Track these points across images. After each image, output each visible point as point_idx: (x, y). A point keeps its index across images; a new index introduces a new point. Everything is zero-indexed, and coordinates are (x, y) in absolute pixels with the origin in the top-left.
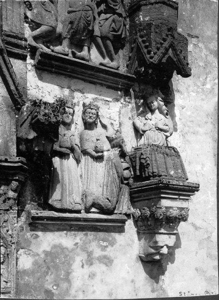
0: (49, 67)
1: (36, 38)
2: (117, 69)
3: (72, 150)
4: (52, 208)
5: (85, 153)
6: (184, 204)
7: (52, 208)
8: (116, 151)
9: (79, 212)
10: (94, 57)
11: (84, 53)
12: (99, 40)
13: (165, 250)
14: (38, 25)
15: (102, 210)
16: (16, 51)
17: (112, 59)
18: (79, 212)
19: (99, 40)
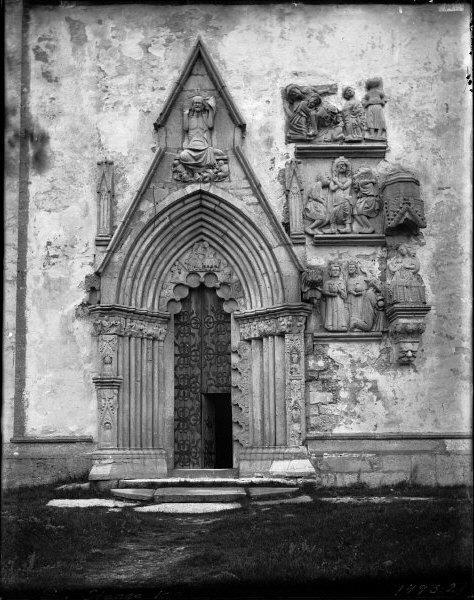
0: (319, 243)
1: (313, 229)
2: (373, 232)
3: (339, 293)
4: (327, 331)
5: (349, 293)
6: (420, 321)
7: (327, 331)
8: (371, 290)
9: (345, 332)
10: (355, 229)
11: (348, 228)
12: (358, 218)
13: (410, 354)
14: (313, 221)
15: (363, 330)
16: (299, 241)
17: (368, 226)
18: (345, 332)
19: (358, 218)
